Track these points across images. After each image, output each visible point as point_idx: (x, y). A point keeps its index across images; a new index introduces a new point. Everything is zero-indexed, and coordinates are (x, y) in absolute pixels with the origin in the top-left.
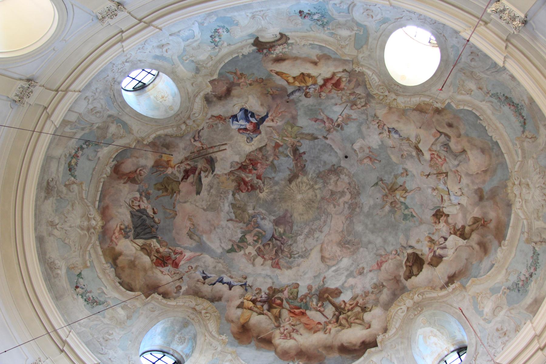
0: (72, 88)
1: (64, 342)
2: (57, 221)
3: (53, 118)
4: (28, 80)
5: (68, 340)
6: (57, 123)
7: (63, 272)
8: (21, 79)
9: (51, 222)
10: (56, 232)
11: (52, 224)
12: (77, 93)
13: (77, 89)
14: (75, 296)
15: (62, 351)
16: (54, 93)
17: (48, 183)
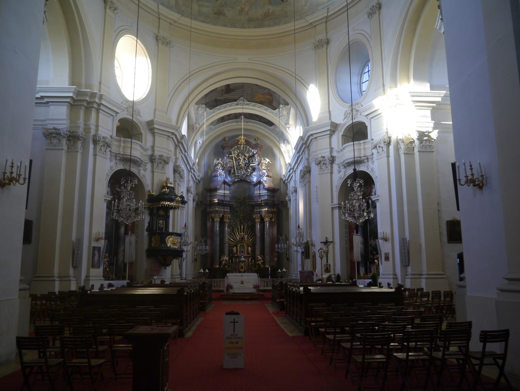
0: (157, 11)
1: (310, 24)
2: (239, 8)
3: (176, 19)
4: (157, 40)
5: (310, 22)
6: (179, 16)
7: (271, 8)
8: (158, 45)
9: (240, 11)
10: (246, 9)
11: (241, 11)
12: (160, 7)
13: (156, 6)
14: (288, 3)
15: (315, 26)
16: (161, 21)
17: (215, 14)
